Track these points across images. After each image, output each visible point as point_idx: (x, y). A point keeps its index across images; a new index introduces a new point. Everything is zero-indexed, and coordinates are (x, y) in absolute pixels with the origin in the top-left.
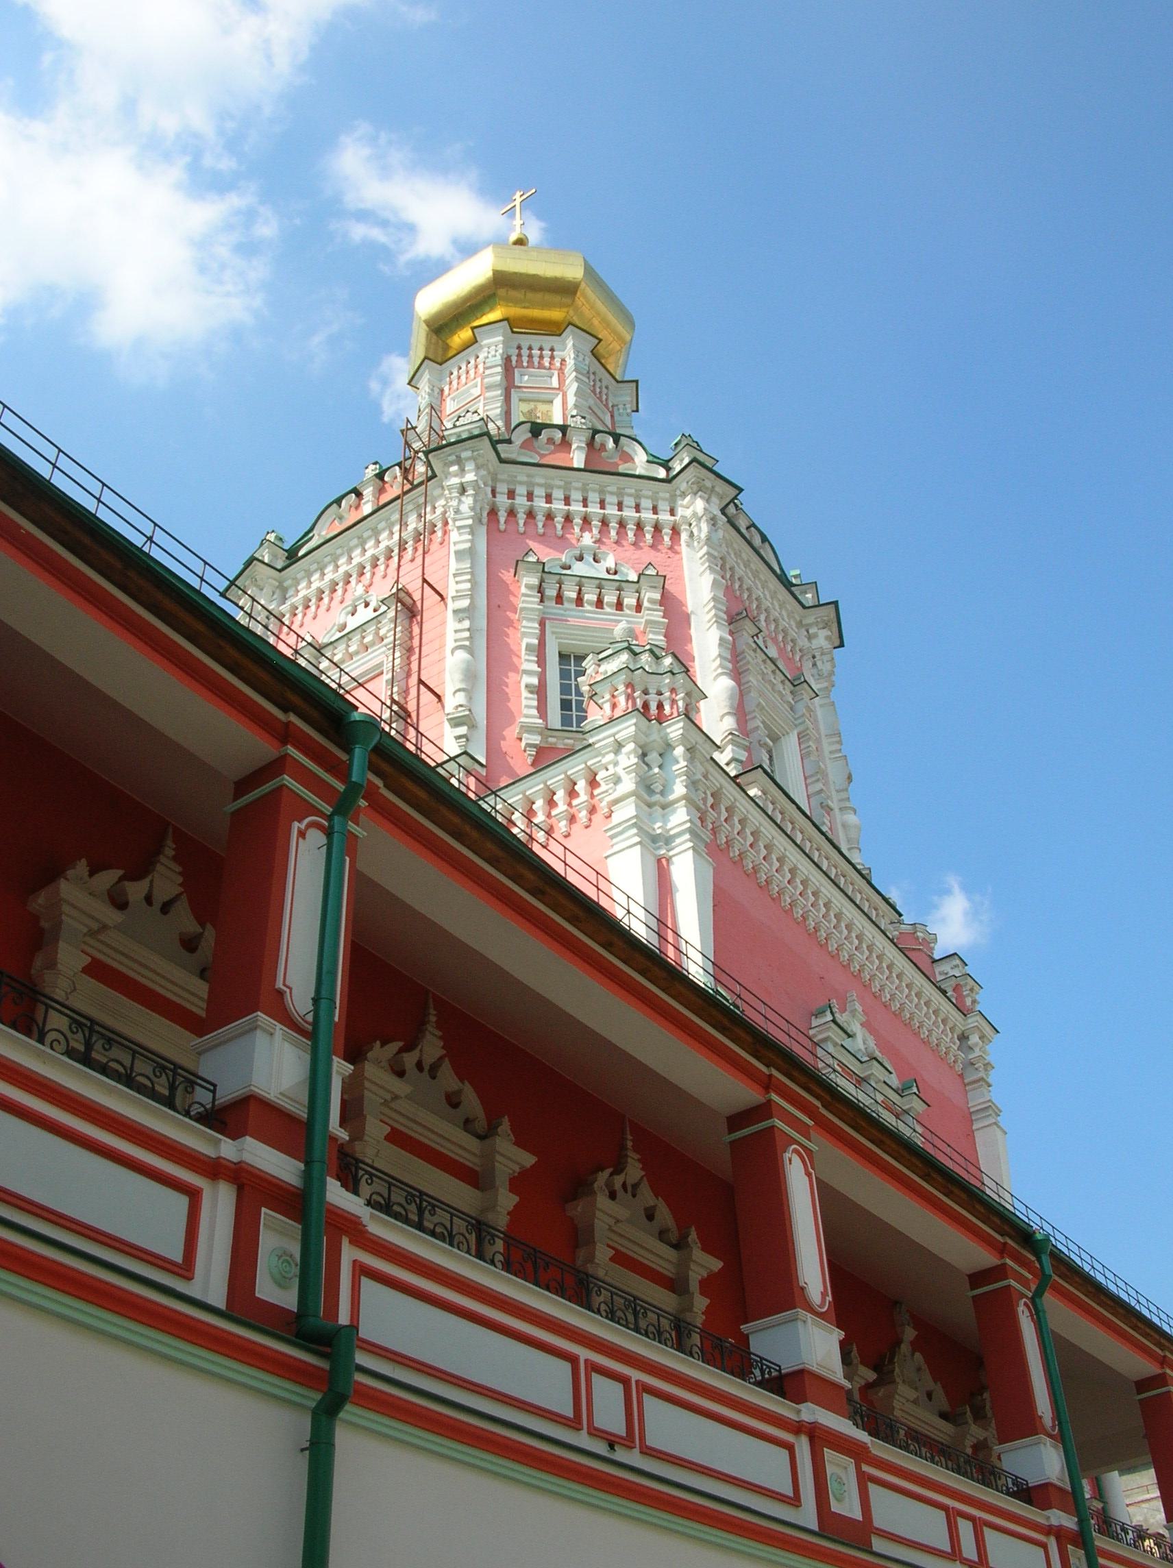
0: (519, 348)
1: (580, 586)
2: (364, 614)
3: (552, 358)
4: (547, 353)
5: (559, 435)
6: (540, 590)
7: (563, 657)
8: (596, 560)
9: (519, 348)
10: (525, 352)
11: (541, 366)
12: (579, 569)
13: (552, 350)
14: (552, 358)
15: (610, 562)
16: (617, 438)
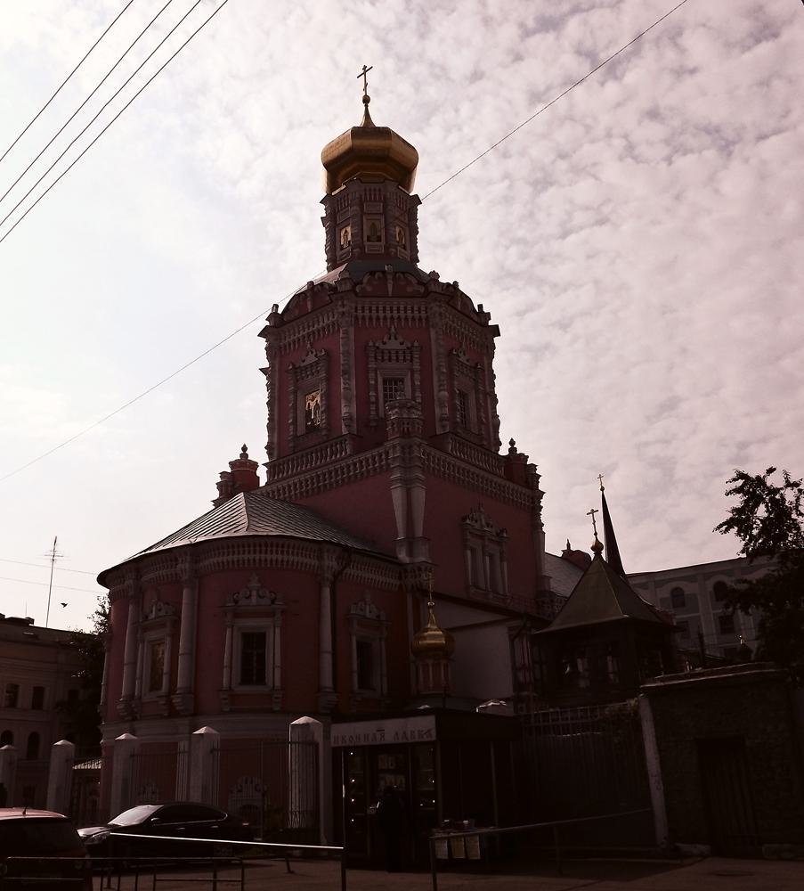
0: (365, 190)
1: (390, 353)
2: (311, 359)
3: (380, 194)
4: (377, 193)
5: (381, 275)
6: (376, 359)
7: (385, 382)
8: (396, 339)
9: (365, 190)
10: (368, 193)
11: (375, 201)
12: (388, 346)
13: (380, 190)
14: (380, 194)
15: (401, 340)
16: (403, 273)
